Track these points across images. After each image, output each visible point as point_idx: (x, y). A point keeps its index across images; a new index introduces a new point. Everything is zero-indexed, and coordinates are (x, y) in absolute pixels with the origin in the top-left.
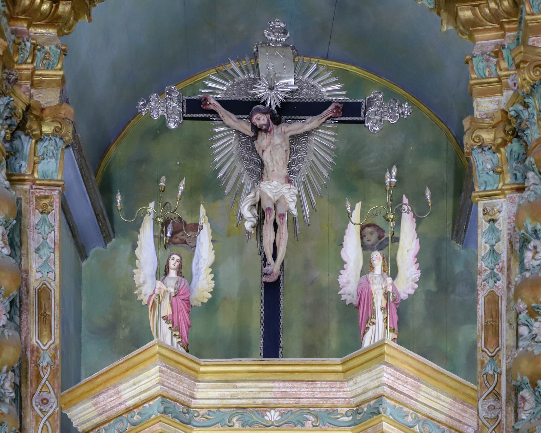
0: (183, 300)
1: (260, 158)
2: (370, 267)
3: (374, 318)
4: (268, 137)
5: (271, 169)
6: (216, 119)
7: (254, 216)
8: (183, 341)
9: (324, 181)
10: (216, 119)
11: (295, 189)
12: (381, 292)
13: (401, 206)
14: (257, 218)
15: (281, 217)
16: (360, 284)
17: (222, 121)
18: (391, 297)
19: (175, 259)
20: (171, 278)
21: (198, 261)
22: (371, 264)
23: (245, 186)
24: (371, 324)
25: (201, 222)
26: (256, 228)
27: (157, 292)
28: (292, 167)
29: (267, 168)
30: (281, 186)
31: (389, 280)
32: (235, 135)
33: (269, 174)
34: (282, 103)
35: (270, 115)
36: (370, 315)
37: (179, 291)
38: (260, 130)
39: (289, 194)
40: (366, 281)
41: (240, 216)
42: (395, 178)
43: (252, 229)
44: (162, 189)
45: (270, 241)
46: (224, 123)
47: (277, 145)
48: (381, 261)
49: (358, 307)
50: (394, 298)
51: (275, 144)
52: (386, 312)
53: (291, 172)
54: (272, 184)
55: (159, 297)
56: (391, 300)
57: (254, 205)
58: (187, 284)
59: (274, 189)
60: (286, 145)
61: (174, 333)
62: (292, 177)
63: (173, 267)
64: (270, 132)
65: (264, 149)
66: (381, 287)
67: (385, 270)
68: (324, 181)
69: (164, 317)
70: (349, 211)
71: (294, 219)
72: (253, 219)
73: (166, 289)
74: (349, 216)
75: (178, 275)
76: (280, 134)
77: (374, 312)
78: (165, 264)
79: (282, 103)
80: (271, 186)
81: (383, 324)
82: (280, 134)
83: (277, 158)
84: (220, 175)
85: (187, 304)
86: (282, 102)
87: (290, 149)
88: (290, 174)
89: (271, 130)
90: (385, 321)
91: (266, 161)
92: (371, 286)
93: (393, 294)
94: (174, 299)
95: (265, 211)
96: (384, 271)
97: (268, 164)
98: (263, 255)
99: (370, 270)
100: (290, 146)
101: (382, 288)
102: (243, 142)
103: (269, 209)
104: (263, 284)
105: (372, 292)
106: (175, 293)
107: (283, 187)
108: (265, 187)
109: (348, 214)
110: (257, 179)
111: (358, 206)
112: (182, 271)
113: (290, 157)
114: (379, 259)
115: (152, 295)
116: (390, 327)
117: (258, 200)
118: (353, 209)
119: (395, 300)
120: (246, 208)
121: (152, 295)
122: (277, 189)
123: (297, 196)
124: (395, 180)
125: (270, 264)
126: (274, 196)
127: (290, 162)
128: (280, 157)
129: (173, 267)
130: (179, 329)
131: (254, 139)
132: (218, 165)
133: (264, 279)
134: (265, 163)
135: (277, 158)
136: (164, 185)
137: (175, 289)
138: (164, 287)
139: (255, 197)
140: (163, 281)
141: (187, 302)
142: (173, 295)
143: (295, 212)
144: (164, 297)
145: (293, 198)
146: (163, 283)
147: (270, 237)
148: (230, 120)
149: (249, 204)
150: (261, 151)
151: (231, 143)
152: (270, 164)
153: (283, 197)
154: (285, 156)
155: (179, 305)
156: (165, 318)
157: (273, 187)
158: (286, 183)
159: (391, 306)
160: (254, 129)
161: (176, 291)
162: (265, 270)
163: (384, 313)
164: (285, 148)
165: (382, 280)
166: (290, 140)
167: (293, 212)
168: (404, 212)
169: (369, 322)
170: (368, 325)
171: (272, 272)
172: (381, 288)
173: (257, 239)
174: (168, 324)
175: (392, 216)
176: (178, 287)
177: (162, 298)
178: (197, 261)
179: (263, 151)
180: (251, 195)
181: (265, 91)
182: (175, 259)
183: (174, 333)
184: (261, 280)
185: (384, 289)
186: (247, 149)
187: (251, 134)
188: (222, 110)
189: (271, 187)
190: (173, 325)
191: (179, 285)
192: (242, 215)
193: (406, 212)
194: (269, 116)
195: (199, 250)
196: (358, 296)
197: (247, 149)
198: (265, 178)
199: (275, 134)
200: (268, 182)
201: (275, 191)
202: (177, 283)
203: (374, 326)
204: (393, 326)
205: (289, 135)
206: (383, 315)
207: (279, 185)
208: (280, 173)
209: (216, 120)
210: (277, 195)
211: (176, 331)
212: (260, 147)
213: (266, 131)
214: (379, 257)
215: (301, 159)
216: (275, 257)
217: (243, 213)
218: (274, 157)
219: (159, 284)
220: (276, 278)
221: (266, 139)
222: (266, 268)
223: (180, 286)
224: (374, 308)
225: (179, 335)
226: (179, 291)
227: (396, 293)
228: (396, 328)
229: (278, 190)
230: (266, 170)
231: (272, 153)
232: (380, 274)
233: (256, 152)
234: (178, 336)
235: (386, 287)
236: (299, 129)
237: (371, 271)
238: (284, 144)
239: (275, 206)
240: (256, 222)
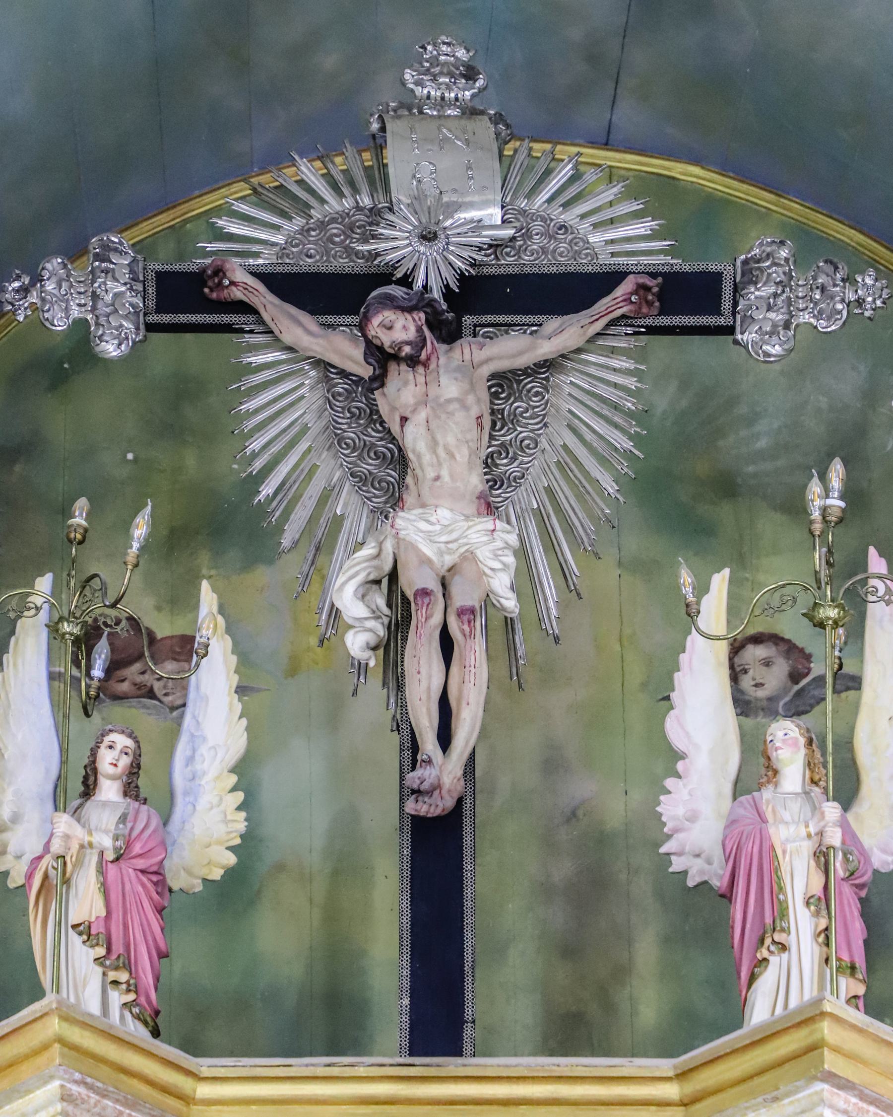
0: (143, 871)
1: (393, 440)
2: (763, 771)
3: (782, 930)
4: (421, 379)
5: (431, 474)
6: (252, 327)
7: (376, 615)
8: (143, 1000)
9: (603, 506)
10: (252, 327)
11: (508, 532)
12: (807, 848)
13: (864, 582)
14: (386, 621)
15: (465, 618)
16: (732, 823)
17: (272, 332)
18: (838, 865)
19: (119, 747)
20: (105, 804)
21: (194, 750)
22: (769, 759)
23: (347, 524)
24: (772, 948)
25: (204, 632)
26: (381, 652)
27: (56, 846)
28: (497, 466)
29: (418, 471)
30: (465, 524)
31: (832, 810)
32: (313, 373)
33: (425, 491)
34: (462, 278)
35: (426, 313)
36: (768, 920)
37: (129, 844)
38: (396, 357)
39: (491, 547)
40: (751, 814)
41: (330, 615)
42: (842, 498)
43: (371, 653)
44: (79, 536)
45: (429, 688)
46: (277, 339)
47: (449, 401)
48: (803, 751)
49: (727, 896)
50: (851, 867)
51: (442, 400)
52: (824, 912)
53: (495, 483)
54: (433, 519)
55: (65, 863)
56: (841, 873)
57: (378, 582)
58: (155, 822)
59: (440, 534)
60: (479, 401)
61: (112, 975)
62: (499, 496)
63: (111, 770)
64: (426, 365)
65: (407, 414)
66: (803, 832)
67: (816, 778)
68: (603, 506)
69: (79, 925)
70: (691, 598)
71: (509, 624)
72: (371, 624)
73: (87, 839)
74: (691, 613)
75: (125, 794)
76: (458, 369)
77: (781, 911)
78: (86, 761)
79: (462, 278)
80: (432, 524)
81: (817, 949)
82: (458, 369)
83: (451, 440)
84: (267, 490)
85: (156, 884)
86: (462, 274)
87: (493, 412)
88: (491, 488)
89: (428, 359)
90: (821, 939)
91: (414, 451)
92: (772, 830)
93: (845, 855)
94: (112, 870)
95: (411, 599)
96: (813, 782)
97: (419, 457)
98: (406, 732)
99: (764, 780)
100: (492, 403)
101: (809, 836)
102: (340, 394)
103: (425, 593)
104: (408, 822)
105: (772, 847)
106: (116, 849)
107: (469, 528)
108: (410, 527)
109: (687, 606)
110: (386, 502)
111: (720, 581)
112: (142, 781)
113: (491, 437)
114: (795, 744)
115: (40, 858)
116: (839, 959)
117: (388, 567)
118: (702, 589)
119: (852, 874)
120: (351, 589)
121: (40, 858)
122: (452, 531)
123: (516, 553)
124: (842, 504)
125: (429, 762)
126: (441, 553)
127: (492, 453)
128: (460, 436)
129: (111, 770)
130: (128, 966)
131: (375, 385)
132: (258, 464)
133: (411, 807)
134: (411, 455)
135: (451, 440)
136: (84, 523)
137: (116, 838)
138: (79, 833)
139: (378, 555)
140: (76, 813)
141: (155, 878)
142: (110, 856)
143: (510, 603)
144: (79, 863)
145: (503, 559)
146: (78, 820)
147: (430, 677)
148: (299, 331)
149: (361, 578)
150: (398, 419)
151: (302, 397)
152: (427, 458)
153: (470, 556)
154: (474, 433)
155: (128, 887)
156: (85, 930)
157: (438, 527)
158: (479, 514)
159: (841, 893)
160: (372, 355)
161: (118, 843)
162: (413, 778)
163: (817, 914)
164: (475, 412)
165: (808, 808)
166: (490, 387)
167: (503, 601)
168: (874, 598)
169: (768, 941)
170: (764, 953)
171: (437, 787)
172: (805, 834)
173: (385, 684)
174: (92, 946)
175: (833, 613)
176: (127, 832)
177: (74, 866)
178: (189, 753)
179: (404, 420)
180: (368, 551)
181: (410, 244)
182: (119, 747)
183: (112, 975)
184: (402, 809)
185: (816, 839)
186: (353, 415)
187: (366, 371)
188: (271, 303)
189: (430, 528)
190: (109, 950)
191: (129, 825)
192: (335, 613)
193: (882, 599)
194: (422, 315)
195: (194, 717)
196: (727, 861)
197: (353, 415)
198: (409, 499)
199: (441, 371)
200: (420, 511)
201: (444, 538)
202: (123, 819)
203: (785, 956)
204: (851, 956)
205: (486, 370)
206: (814, 920)
207: (456, 522)
208: (458, 484)
209: (251, 332)
210: (450, 552)
211: (117, 968)
212: (393, 409)
213: (413, 361)
214: (796, 738)
215: (527, 442)
216: (445, 738)
217: (338, 604)
218: (439, 437)
219: (64, 822)
220: (449, 803)
221: (411, 386)
222: (418, 773)
223: (132, 829)
224: (781, 897)
225: (128, 983)
226: (129, 844)
227: (856, 852)
228: (860, 962)
229: (454, 536)
230: (415, 477)
231: (433, 424)
232: (799, 789)
233: (382, 423)
234: (124, 987)
235: (821, 834)
236: (521, 353)
237: (769, 782)
238: (471, 399)
239: (444, 585)
240: (382, 632)
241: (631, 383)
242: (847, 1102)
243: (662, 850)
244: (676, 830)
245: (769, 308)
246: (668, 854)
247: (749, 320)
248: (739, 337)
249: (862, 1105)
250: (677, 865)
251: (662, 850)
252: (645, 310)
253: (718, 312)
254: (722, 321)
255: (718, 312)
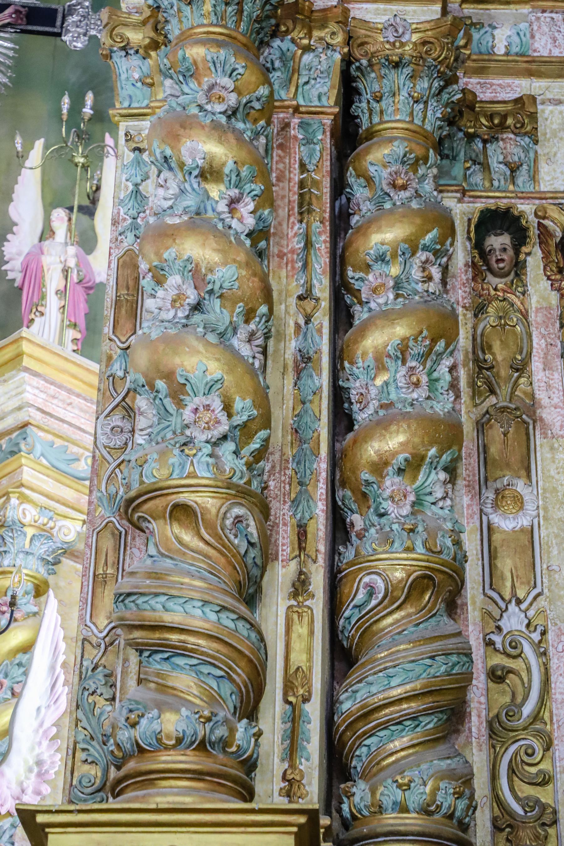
3: (42, 305)
24: (37, 314)
42: (91, 109)
66: (58, 260)
77: (43, 297)
124: (92, 112)
203: (43, 318)
241: (11, 53)
242: (38, 383)
243: (4, 268)
244: (11, 259)
245: (77, 27)
246: (6, 271)
247: (68, 31)
248: (63, 38)
249: (46, 384)
250: (10, 276)
251: (4, 268)
252: (20, 22)
253: (54, 26)
254: (56, 30)
255: (54, 26)
